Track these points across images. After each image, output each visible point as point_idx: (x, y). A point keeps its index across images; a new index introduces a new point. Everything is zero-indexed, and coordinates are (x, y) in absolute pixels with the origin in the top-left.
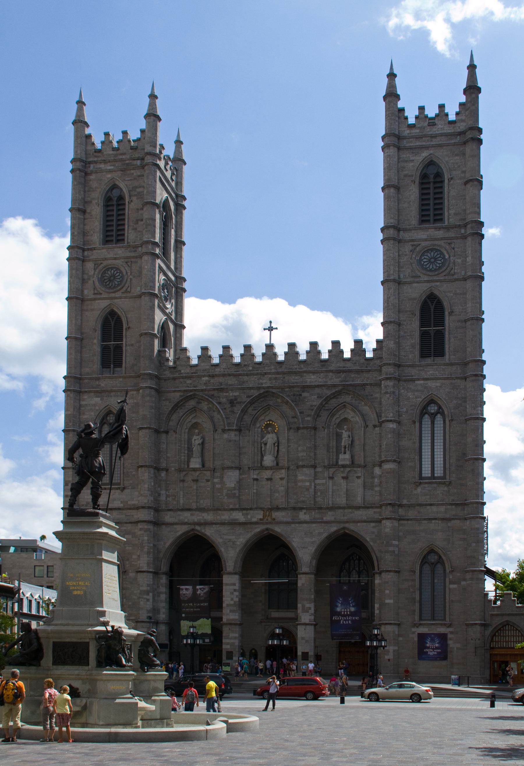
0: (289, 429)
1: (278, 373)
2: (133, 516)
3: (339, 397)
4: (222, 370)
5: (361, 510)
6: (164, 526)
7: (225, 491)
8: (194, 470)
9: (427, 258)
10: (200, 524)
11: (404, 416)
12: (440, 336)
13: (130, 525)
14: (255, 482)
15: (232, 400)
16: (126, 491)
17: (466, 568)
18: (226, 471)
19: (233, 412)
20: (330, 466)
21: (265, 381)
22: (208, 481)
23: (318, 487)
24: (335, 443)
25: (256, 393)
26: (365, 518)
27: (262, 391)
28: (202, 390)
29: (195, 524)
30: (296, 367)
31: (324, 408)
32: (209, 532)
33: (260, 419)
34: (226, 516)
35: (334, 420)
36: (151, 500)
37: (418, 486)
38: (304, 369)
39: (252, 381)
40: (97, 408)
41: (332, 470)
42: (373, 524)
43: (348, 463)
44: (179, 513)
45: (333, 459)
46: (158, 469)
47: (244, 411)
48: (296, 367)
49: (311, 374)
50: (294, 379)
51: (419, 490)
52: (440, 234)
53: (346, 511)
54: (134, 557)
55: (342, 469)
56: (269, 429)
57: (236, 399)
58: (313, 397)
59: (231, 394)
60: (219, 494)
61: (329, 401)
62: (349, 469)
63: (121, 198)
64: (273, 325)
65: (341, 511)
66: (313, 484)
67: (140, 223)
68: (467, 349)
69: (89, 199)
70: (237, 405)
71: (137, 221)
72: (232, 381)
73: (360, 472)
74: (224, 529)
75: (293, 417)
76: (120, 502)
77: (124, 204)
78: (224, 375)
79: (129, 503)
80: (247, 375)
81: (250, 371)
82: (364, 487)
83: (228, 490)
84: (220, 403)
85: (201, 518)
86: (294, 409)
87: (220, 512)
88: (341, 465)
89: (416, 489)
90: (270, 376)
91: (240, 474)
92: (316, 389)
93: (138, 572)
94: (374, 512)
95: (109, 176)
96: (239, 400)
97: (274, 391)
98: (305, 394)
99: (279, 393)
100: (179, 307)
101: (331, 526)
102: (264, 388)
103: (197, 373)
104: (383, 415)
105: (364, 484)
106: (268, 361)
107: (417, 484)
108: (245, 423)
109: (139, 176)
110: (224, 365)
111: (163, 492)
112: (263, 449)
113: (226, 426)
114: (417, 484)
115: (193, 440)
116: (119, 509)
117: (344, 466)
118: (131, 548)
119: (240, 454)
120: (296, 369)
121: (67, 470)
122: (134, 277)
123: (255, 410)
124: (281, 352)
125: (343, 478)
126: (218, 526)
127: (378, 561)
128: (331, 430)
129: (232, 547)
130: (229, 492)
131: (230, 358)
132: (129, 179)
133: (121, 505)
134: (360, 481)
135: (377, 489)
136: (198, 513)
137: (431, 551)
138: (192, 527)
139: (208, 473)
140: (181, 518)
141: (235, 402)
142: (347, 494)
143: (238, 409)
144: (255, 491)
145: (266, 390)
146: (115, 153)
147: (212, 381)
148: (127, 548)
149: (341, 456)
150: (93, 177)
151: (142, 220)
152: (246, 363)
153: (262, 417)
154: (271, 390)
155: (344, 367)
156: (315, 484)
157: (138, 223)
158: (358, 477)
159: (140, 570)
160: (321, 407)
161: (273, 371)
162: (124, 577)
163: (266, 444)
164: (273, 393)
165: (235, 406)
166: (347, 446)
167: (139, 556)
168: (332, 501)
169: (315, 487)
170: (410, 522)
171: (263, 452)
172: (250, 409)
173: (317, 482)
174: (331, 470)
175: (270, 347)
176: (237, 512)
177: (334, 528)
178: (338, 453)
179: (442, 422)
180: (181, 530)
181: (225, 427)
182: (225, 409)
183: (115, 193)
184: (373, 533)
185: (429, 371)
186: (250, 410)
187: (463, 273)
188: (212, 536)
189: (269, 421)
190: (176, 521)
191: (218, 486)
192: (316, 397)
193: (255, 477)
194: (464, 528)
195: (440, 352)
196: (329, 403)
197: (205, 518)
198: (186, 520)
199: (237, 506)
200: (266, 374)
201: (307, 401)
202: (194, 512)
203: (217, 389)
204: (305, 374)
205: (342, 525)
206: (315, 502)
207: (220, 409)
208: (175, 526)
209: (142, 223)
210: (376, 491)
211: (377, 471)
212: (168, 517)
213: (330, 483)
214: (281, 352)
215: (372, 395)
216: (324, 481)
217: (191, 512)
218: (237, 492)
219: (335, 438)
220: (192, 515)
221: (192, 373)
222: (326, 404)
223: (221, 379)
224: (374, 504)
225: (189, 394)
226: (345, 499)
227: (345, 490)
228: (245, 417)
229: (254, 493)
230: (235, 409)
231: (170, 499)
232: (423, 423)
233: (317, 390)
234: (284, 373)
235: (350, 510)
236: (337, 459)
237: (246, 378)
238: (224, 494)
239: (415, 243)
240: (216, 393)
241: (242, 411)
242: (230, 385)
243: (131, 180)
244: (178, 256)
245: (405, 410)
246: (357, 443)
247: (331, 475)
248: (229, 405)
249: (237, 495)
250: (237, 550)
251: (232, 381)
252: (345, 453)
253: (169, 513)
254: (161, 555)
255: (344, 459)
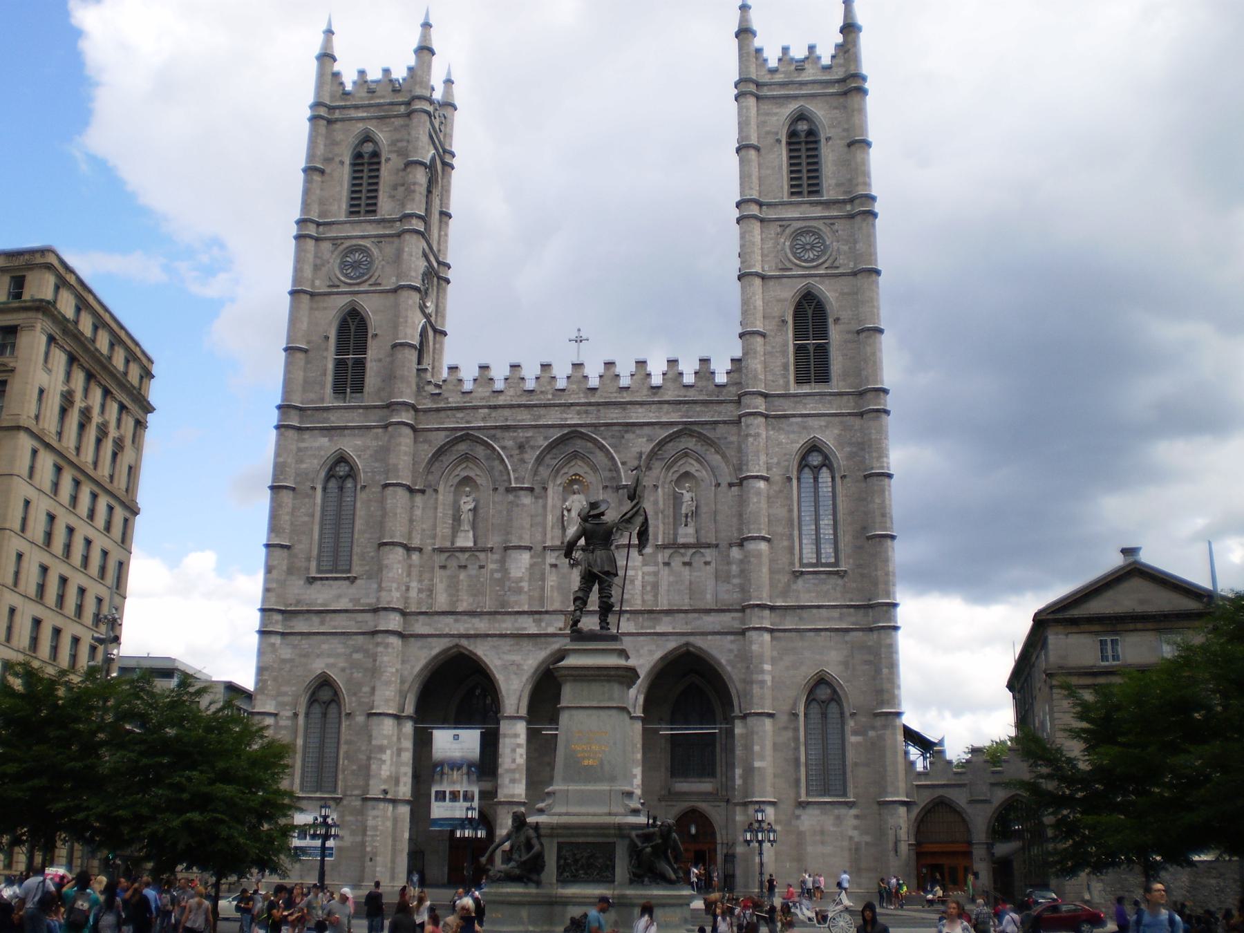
0: (605, 487)
1: (590, 404)
2: (367, 622)
3: (678, 440)
4: (508, 398)
5: (712, 614)
6: (413, 639)
7: (507, 583)
8: (463, 550)
9: (801, 243)
10: (468, 636)
11: (774, 470)
12: (823, 352)
13: (360, 638)
14: (554, 569)
15: (522, 443)
16: (358, 582)
17: (876, 709)
18: (509, 552)
19: (523, 461)
20: (664, 547)
21: (570, 416)
22: (482, 567)
23: (646, 578)
24: (671, 510)
25: (558, 434)
26: (718, 628)
27: (566, 431)
28: (479, 428)
29: (461, 636)
30: (615, 395)
31: (655, 457)
32: (482, 651)
33: (562, 472)
34: (507, 625)
35: (670, 474)
36: (397, 598)
37: (797, 577)
38: (628, 399)
39: (553, 417)
40: (322, 453)
41: (668, 552)
42: (730, 638)
43: (692, 540)
44: (436, 618)
45: (669, 534)
46: (408, 549)
47: (540, 460)
48: (615, 395)
49: (637, 406)
50: (614, 416)
51: (800, 582)
52: (818, 212)
53: (691, 616)
54: (366, 689)
55: (682, 551)
56: (576, 487)
57: (528, 442)
58: (640, 440)
59: (521, 435)
60: (498, 588)
61: (663, 446)
62: (694, 550)
63: (376, 154)
64: (584, 335)
65: (682, 615)
66: (640, 573)
67: (401, 189)
68: (863, 372)
69: (330, 156)
70: (529, 450)
71: (395, 187)
72: (525, 417)
73: (709, 554)
74: (506, 644)
75: (610, 470)
76: (347, 600)
77: (379, 163)
78: (511, 406)
79: (362, 601)
80: (545, 406)
81: (549, 400)
82: (716, 577)
83: (513, 582)
84: (503, 448)
85: (470, 625)
86: (613, 458)
87: (499, 617)
88: (682, 544)
89: (795, 582)
90: (578, 408)
91: (532, 557)
92: (646, 428)
93: (370, 715)
94: (733, 618)
95: (361, 126)
96: (532, 443)
97: (583, 430)
98: (627, 436)
99: (590, 433)
100: (440, 304)
101: (667, 640)
102: (569, 426)
103: (471, 402)
104: (744, 467)
105: (716, 573)
106: (574, 387)
107: (798, 574)
108: (539, 479)
109: (402, 126)
110: (511, 392)
111: (414, 585)
112: (565, 518)
113: (513, 482)
114: (798, 574)
115: (462, 502)
116: (346, 611)
117: (686, 546)
118: (360, 675)
119: (531, 526)
120: (616, 397)
121: (272, 549)
122: (388, 263)
123: (555, 458)
124: (593, 372)
125: (685, 564)
126: (495, 639)
127: (739, 697)
128: (666, 490)
129: (516, 674)
130: (513, 585)
131: (520, 381)
132: (387, 129)
133: (350, 606)
134: (710, 569)
135: (736, 581)
136: (466, 617)
137: (821, 681)
138: (456, 641)
139: (482, 556)
140: (440, 626)
141: (527, 446)
142: (690, 589)
143: (531, 456)
144: (552, 583)
145: (573, 429)
146: (370, 95)
147: (494, 414)
148: (355, 675)
149: (682, 530)
150: (338, 126)
151: (403, 185)
152: (544, 389)
153: (565, 470)
154: (579, 429)
155: (685, 396)
156: (643, 573)
157: (396, 189)
158: (707, 563)
159: (374, 711)
160: (653, 455)
161: (583, 400)
162: (348, 723)
163: (569, 511)
164: (582, 433)
165: (526, 452)
166: (690, 514)
167: (373, 689)
168: (669, 600)
169: (643, 578)
170: (787, 634)
171: (565, 523)
172: (549, 456)
173: (646, 569)
174: (666, 551)
175: (578, 366)
176: (526, 616)
177: (672, 644)
178: (676, 526)
179: (830, 480)
180: (438, 647)
181: (511, 484)
182: (511, 456)
183: (368, 148)
184: (731, 651)
185: (809, 404)
186: (548, 459)
187: (851, 265)
188: (485, 655)
189: (575, 475)
190: (432, 631)
191: (498, 575)
192: (645, 439)
193: (553, 561)
194: (869, 644)
195: (823, 376)
196: (663, 448)
197: (476, 626)
198: (446, 631)
199: (526, 608)
200: (572, 405)
201: (632, 447)
202: (459, 617)
203: (501, 427)
204: (629, 406)
205: (684, 640)
206: (643, 601)
207: (504, 457)
208: (430, 640)
209: (403, 188)
210: (734, 585)
211: (735, 553)
212: (420, 627)
213: (665, 572)
214: (593, 372)
215: (726, 438)
216: (657, 568)
217: (454, 617)
218: (525, 585)
219: (672, 502)
220: (456, 621)
221: (465, 402)
222: (659, 450)
223: (507, 412)
224: (732, 605)
225: (459, 434)
226: (688, 596)
227: (688, 583)
228: (541, 469)
229: (551, 586)
230: (526, 456)
231: (423, 596)
232: (802, 480)
233: (647, 430)
234: (598, 404)
235: (696, 615)
236: (675, 535)
237: (542, 411)
238: (506, 589)
239: (784, 223)
240: (499, 433)
241: (537, 459)
242: (519, 421)
243: (390, 131)
244: (443, 233)
245: (775, 460)
246: (704, 509)
247: (666, 560)
248: (517, 452)
249: (526, 589)
250: (524, 679)
251: (525, 417)
252: (686, 525)
253: (421, 618)
254: (406, 686)
255: (686, 535)
